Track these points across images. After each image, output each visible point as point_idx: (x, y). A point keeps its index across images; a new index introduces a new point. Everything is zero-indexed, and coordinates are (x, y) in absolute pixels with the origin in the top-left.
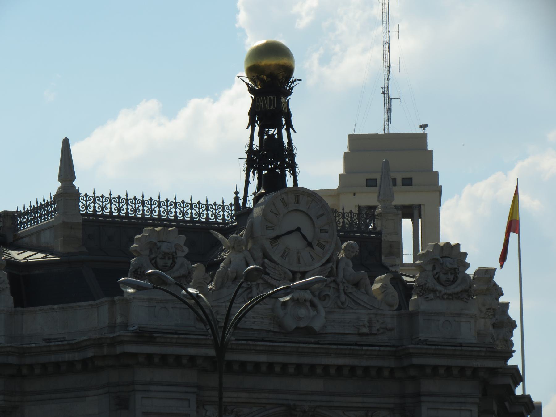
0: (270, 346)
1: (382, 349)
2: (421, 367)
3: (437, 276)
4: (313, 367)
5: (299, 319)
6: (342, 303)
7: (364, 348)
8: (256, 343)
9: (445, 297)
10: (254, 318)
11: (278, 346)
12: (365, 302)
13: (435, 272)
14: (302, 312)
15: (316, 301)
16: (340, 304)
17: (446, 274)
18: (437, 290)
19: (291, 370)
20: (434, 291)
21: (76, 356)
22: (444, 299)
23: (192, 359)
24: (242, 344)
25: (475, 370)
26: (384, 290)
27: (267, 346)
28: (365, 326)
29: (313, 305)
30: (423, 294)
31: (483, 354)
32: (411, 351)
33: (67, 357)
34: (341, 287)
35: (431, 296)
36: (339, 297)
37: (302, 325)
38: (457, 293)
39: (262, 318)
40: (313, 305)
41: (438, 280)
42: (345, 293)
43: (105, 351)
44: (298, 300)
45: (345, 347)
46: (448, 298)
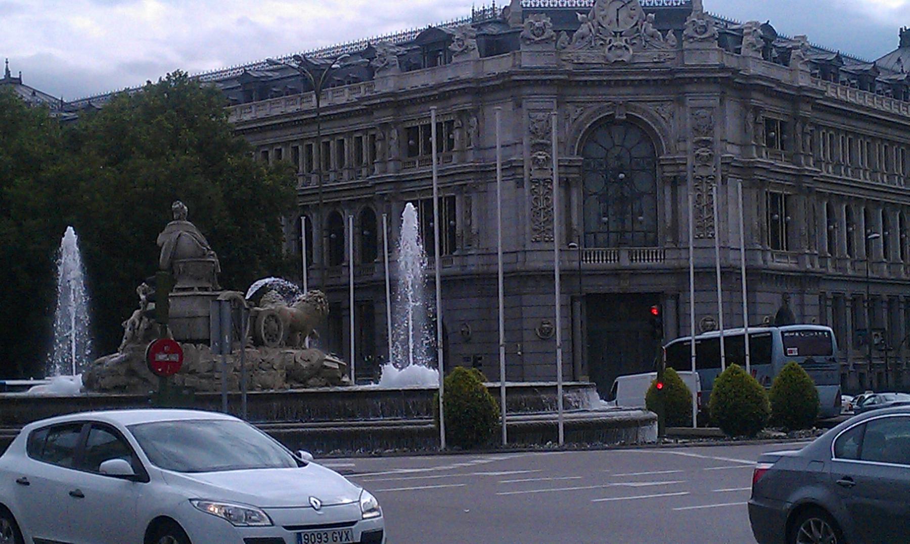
19: (613, 83)
29: (627, 49)
40: (627, 49)
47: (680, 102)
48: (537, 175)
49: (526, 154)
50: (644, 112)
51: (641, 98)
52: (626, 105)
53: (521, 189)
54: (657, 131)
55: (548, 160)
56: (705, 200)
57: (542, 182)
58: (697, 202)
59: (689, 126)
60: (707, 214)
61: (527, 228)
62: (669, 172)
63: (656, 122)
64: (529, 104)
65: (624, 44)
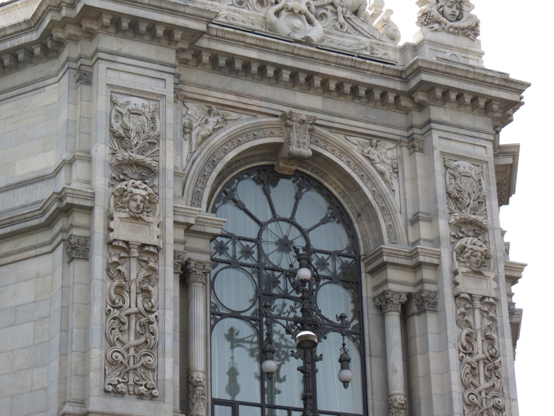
0: (261, 40)
1: (386, 65)
2: (430, 88)
3: (441, 10)
4: (310, 76)
5: (295, 29)
6: (341, 27)
7: (367, 61)
8: (245, 33)
9: (452, 30)
10: (243, 21)
11: (272, 41)
12: (365, 31)
13: (439, 5)
14: (297, 22)
15: (312, 17)
16: (339, 26)
17: (450, 7)
18: (443, 22)
19: (286, 75)
20: (440, 23)
21: (34, 36)
22: (450, 33)
23: (170, 30)
24: (228, 32)
25: (490, 101)
26: (384, 24)
27: (258, 39)
28: (366, 49)
30: (428, 24)
31: (497, 82)
32: (420, 64)
33: (24, 39)
34: (340, 9)
35: (436, 26)
36: (337, 20)
37: (298, 36)
38: (463, 29)
39: (253, 24)
41: (442, 13)
42: (344, 17)
43: (64, 12)
44: (292, 11)
45: (347, 56)
46: (453, 33)
47: (414, 142)
48: (123, 231)
49: (101, 182)
50: (344, 152)
51: (338, 122)
52: (312, 126)
53: (78, 266)
54: (370, 197)
55: (150, 203)
56: (479, 345)
57: (135, 252)
58: (467, 350)
59: (441, 191)
60: (487, 379)
61: (97, 355)
62: (399, 282)
63: (369, 178)
64: (111, 73)
65: (304, 8)
